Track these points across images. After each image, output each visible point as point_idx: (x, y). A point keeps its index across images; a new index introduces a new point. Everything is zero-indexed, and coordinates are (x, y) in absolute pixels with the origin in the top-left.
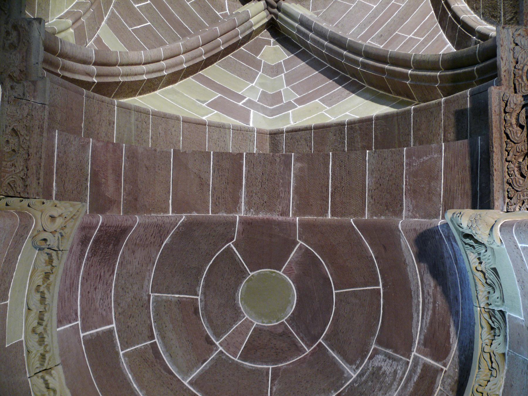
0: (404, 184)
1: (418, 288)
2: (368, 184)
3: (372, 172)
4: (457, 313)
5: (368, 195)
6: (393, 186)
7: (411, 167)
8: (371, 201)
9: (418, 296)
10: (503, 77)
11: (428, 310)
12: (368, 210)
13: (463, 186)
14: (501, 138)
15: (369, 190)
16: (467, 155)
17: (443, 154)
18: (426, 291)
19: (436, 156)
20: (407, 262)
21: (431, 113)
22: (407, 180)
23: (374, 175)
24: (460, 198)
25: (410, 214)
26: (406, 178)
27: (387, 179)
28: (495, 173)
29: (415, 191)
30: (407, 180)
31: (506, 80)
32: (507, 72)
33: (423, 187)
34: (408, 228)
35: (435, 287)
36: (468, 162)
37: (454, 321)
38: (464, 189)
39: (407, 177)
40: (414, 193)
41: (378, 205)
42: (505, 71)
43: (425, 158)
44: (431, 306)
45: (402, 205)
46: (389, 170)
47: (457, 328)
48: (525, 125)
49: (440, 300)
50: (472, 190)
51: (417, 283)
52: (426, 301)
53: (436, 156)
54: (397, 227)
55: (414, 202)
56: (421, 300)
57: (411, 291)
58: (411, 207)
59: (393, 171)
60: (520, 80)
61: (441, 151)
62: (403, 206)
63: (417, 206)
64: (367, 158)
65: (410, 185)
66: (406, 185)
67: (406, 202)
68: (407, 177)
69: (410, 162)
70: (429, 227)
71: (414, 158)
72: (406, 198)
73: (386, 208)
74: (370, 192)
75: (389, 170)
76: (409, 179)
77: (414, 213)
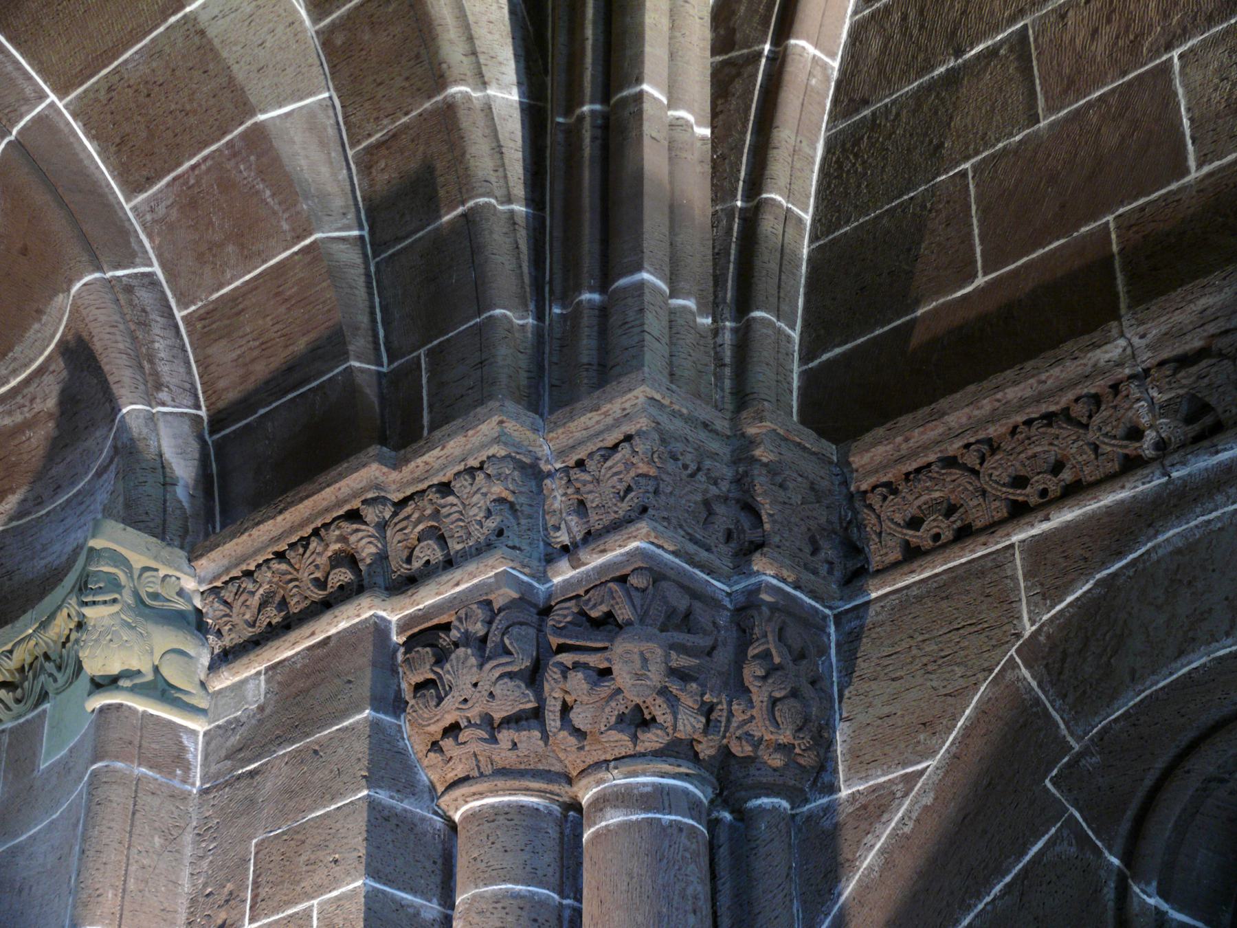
0: (193, 162)
1: (26, 366)
2: (126, 61)
3: (153, 52)
4: (39, 502)
5: (106, 76)
6: (170, 133)
7: (233, 162)
8: (103, 92)
9: (15, 372)
10: (412, 465)
11: (10, 413)
12: (79, 98)
13: (256, 353)
14: (302, 525)
15: (116, 71)
16: (312, 336)
17: (296, 249)
18: (31, 389)
19: (286, 226)
20: (44, 318)
21: (418, 56)
22: (203, 167)
23: (154, 64)
24: (234, 355)
25: (148, 217)
26: (205, 159)
27: (173, 107)
28: (245, 537)
29: (193, 204)
30: (203, 167)
31: (412, 472)
32: (427, 467)
33: (211, 223)
34: (84, 312)
35: (50, 415)
36: (301, 345)
37: (24, 500)
38: (253, 360)
39: (209, 163)
40: (190, 199)
41: (109, 116)
42: (427, 463)
43: (268, 193)
44: (18, 418)
45: (150, 181)
46: (191, 101)
47: (19, 515)
48: (329, 590)
49: (38, 438)
50: (256, 391)
51: (32, 361)
52: (19, 399)
53: (286, 226)
54: (70, 282)
55: (174, 213)
56: (13, 383)
57: (11, 349)
58: (161, 211)
59: (195, 112)
60: (416, 515)
61: (299, 238)
62: (151, 186)
63: (171, 227)
64: (173, 19)
65: (198, 182)
66: (193, 168)
67: (160, 191)
68: (209, 163)
69: (239, 152)
70: (111, 379)
71: (252, 158)
72: (168, 185)
73: (118, 140)
74: (117, 77)
75: (191, 101)
76: (209, 170)
77: (156, 229)
